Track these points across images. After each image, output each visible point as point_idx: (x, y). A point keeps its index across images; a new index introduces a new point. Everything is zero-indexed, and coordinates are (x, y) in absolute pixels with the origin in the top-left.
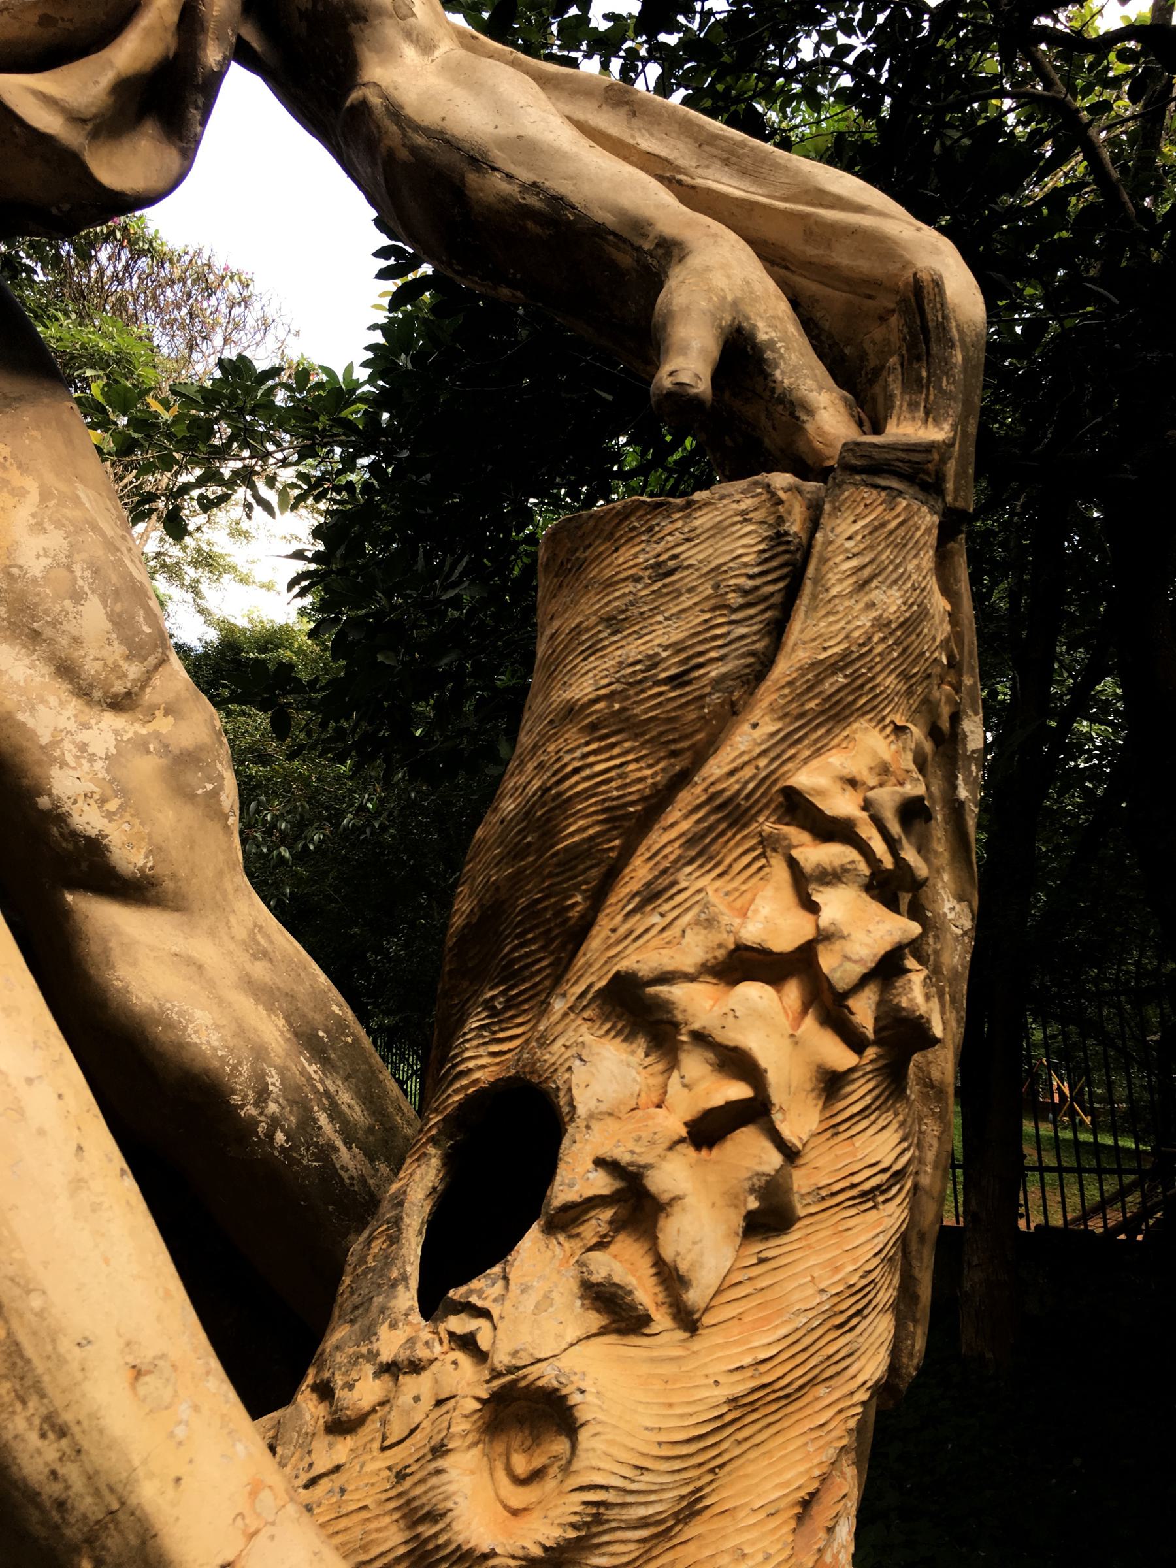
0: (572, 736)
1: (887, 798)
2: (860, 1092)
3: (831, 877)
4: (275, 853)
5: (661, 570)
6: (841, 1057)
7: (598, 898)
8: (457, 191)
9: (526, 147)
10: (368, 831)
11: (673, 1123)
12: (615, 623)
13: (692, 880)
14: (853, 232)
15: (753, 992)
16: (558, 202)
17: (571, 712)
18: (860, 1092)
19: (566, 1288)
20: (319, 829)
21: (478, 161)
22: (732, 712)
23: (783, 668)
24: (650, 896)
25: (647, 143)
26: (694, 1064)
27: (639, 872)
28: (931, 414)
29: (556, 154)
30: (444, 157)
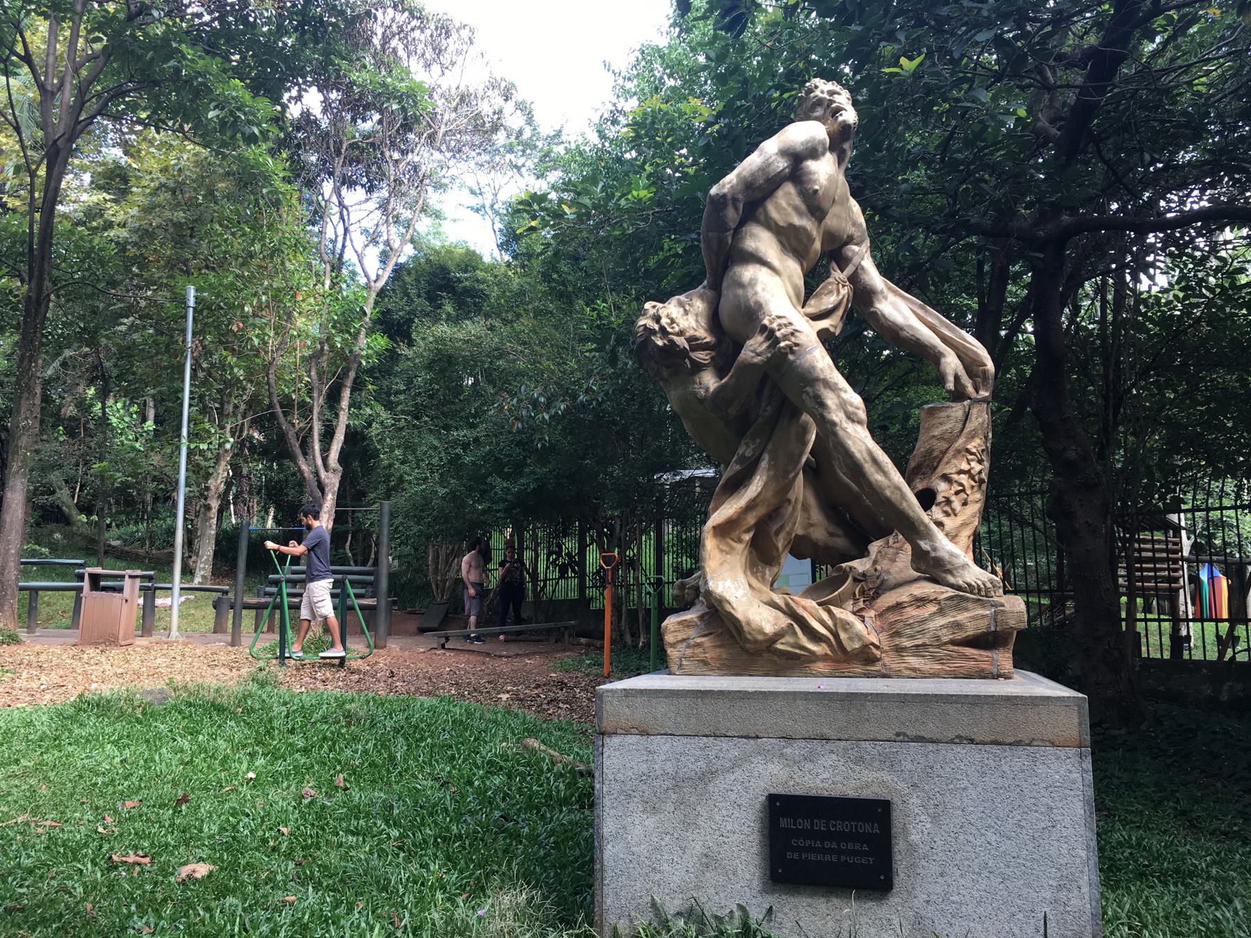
0: (934, 440)
1: (980, 449)
2: (976, 489)
3: (972, 460)
4: (540, 416)
5: (948, 417)
6: (974, 484)
7: (939, 463)
8: (898, 334)
9: (911, 327)
10: (594, 403)
11: (953, 492)
12: (941, 424)
13: (954, 461)
14: (972, 350)
15: (962, 476)
16: (918, 339)
17: (934, 436)
18: (976, 489)
19: (940, 512)
20: (563, 401)
21: (902, 329)
22: (958, 437)
23: (965, 431)
24: (947, 463)
25: (930, 319)
26: (955, 485)
27: (945, 459)
28: (986, 390)
29: (916, 329)
30: (895, 328)
